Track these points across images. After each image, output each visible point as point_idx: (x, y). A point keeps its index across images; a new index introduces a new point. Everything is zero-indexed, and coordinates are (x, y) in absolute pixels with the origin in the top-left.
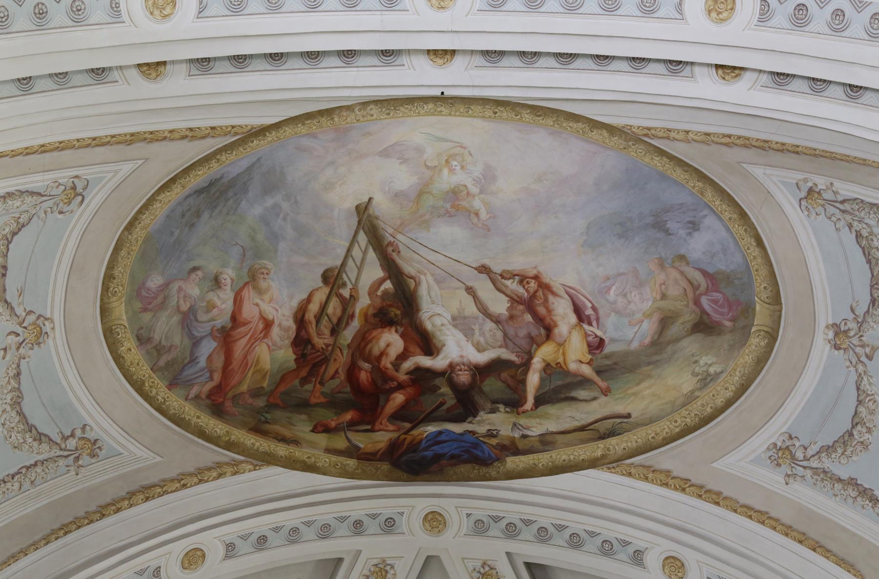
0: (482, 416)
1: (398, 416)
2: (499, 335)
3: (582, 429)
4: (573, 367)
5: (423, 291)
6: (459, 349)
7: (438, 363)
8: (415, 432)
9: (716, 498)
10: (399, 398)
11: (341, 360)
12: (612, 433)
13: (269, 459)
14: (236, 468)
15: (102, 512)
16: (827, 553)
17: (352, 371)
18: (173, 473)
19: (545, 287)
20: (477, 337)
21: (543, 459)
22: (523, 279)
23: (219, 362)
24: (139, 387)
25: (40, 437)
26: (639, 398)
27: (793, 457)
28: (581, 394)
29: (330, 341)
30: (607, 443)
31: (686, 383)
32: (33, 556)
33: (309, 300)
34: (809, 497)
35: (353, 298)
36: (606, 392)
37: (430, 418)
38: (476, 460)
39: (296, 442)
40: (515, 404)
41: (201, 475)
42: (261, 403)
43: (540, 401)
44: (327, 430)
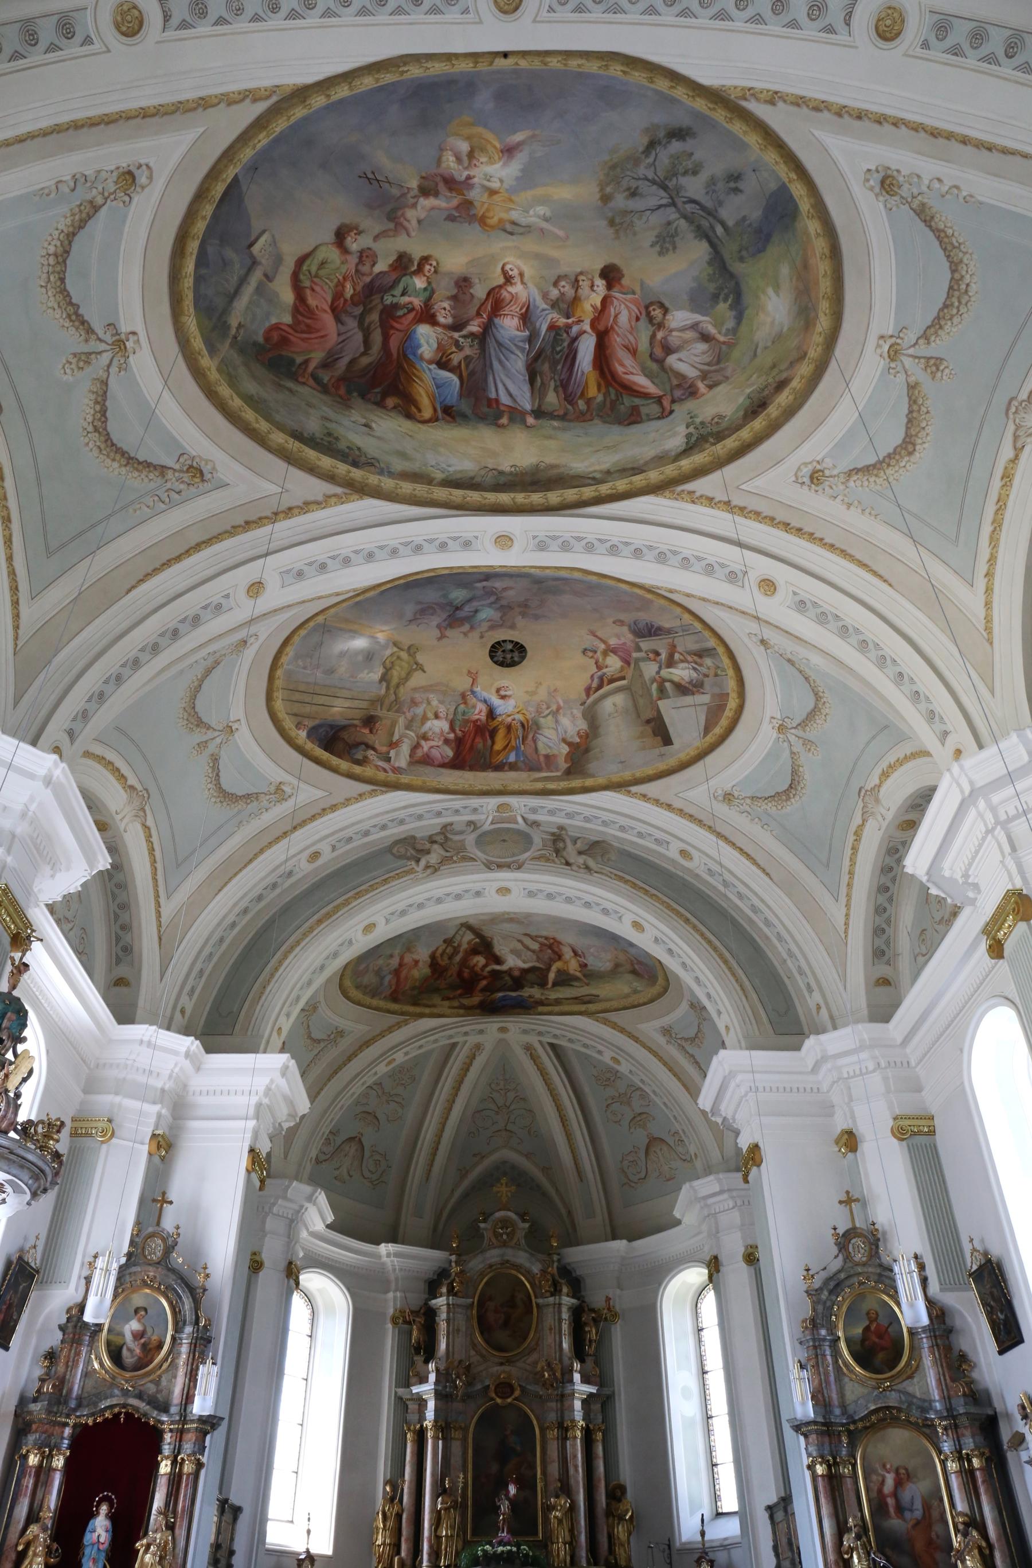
0: (526, 989)
1: (484, 990)
2: (535, 957)
3: (576, 998)
4: (572, 972)
5: (495, 942)
6: (512, 962)
7: (504, 967)
8: (493, 996)
9: (636, 1040)
10: (484, 983)
11: (454, 970)
12: (589, 1002)
13: (422, 1016)
14: (406, 1023)
15: (349, 1059)
16: (679, 1079)
17: (460, 974)
18: (378, 1032)
19: (559, 943)
20: (523, 957)
21: (557, 1009)
22: (546, 938)
23: (394, 982)
24: (359, 1003)
25: (319, 1041)
27: (671, 1035)
28: (575, 984)
29: (447, 962)
30: (585, 1005)
31: (626, 990)
32: (325, 1089)
33: (437, 949)
34: (673, 1051)
35: (459, 946)
36: (587, 985)
37: (499, 990)
38: (523, 1007)
39: (434, 1006)
40: (543, 984)
41: (390, 1030)
42: (415, 992)
43: (554, 985)
44: (448, 999)
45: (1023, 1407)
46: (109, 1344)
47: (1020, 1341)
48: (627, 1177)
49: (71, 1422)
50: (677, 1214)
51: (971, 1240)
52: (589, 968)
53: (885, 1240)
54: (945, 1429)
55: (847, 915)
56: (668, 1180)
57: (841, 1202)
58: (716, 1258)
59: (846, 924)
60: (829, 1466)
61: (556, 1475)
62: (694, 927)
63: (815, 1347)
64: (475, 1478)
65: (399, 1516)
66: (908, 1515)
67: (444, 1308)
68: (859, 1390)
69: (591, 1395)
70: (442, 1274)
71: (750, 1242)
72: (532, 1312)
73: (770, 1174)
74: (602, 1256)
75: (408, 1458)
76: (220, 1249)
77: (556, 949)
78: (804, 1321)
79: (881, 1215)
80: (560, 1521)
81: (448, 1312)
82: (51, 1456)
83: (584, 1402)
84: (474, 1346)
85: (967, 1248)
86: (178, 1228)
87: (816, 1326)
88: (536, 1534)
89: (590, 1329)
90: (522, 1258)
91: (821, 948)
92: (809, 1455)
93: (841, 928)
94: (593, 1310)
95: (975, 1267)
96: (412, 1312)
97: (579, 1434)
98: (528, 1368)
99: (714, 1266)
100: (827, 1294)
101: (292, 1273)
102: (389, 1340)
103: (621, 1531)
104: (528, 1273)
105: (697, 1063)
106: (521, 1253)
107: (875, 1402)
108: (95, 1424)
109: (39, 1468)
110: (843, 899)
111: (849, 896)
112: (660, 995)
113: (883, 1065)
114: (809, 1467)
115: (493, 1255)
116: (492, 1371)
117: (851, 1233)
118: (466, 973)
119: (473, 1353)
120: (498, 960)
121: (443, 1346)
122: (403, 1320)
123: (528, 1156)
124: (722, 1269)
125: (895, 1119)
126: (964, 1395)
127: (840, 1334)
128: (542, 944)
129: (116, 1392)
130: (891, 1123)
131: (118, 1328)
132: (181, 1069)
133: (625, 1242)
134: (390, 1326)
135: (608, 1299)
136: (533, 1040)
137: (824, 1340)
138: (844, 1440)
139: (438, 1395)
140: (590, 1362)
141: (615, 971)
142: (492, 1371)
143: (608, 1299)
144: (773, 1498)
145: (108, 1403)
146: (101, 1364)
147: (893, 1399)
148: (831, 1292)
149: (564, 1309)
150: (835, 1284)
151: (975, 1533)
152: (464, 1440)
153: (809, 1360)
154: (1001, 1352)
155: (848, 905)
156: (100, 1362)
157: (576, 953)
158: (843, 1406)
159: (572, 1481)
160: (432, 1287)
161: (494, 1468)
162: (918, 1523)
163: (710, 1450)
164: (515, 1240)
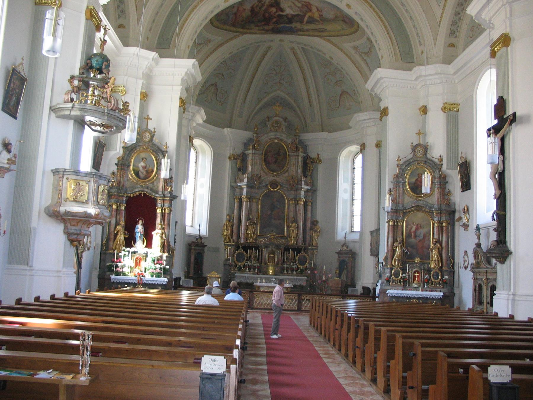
0: (294, 24)
1: (274, 23)
3: (316, 29)
6: (288, 11)
7: (285, 14)
9: (342, 50)
10: (275, 20)
13: (246, 33)
14: (238, 36)
17: (264, 15)
19: (311, 5)
21: (307, 33)
22: (305, 2)
24: (218, 27)
26: (330, 27)
30: (320, 33)
31: (339, 28)
34: (357, 57)
35: (265, 3)
36: (322, 24)
37: (282, 23)
38: (292, 31)
39: (251, 29)
40: (301, 22)
41: (231, 39)
43: (307, 22)
44: (258, 26)
45: (464, 209)
46: (134, 170)
47: (470, 189)
48: (331, 106)
49: (125, 196)
50: (350, 124)
51: (462, 153)
52: (323, 16)
53: (430, 149)
54: (437, 214)
55: (442, 14)
56: (348, 109)
57: (416, 134)
58: (364, 144)
59: (441, 18)
60: (394, 222)
61: (292, 216)
62: (374, 10)
63: (397, 184)
64: (261, 216)
65: (232, 226)
66: (417, 238)
67: (251, 155)
68: (409, 200)
69: (308, 190)
70: (250, 140)
71: (379, 139)
72: (286, 158)
73: (391, 119)
74: (317, 141)
75: (236, 207)
76: (170, 137)
77: (309, 7)
78: (394, 175)
79: (430, 140)
80: (293, 231)
81: (252, 156)
82: (120, 206)
83: (305, 192)
84: (262, 169)
85: (460, 156)
86: (155, 129)
87: (398, 179)
88: (284, 234)
89: (309, 165)
90: (283, 136)
91: (429, 27)
92: (388, 218)
93: (438, 19)
94: (311, 158)
95: (461, 163)
96: (238, 155)
97: (302, 203)
98: (284, 178)
99: (363, 148)
100: (404, 166)
101: (191, 140)
102: (228, 165)
103: (315, 235)
104: (285, 143)
105: (367, 63)
106: (283, 135)
107: (414, 204)
108: (134, 197)
109: (117, 210)
110: (442, 6)
111: (445, 5)
112: (354, 32)
113: (444, 81)
114: (387, 222)
115: (272, 135)
116: (269, 178)
117: (419, 145)
118: (267, 15)
119: (262, 172)
120: (282, 10)
121: (250, 169)
122: (234, 158)
123: (288, 94)
124: (366, 148)
125: (444, 104)
126: (446, 204)
127: (407, 180)
128: (303, 5)
129: (139, 186)
130: (442, 105)
131: (136, 164)
132: (151, 65)
133: (327, 133)
134: (228, 161)
135: (318, 155)
136: (296, 46)
137: (401, 182)
138: (401, 215)
139: (248, 186)
140: (309, 178)
141: (335, 19)
142: (269, 178)
143: (318, 155)
144: (373, 229)
145: (137, 190)
146: (132, 177)
147: (421, 203)
148: (406, 166)
149: (300, 158)
150: (408, 163)
151: (438, 245)
152: (258, 203)
153: (394, 188)
154: (462, 192)
155: (443, 9)
156: (131, 175)
157: (318, 10)
158: (403, 204)
159: (299, 219)
160: (245, 146)
161: (269, 212)
162: (420, 241)
163: (352, 211)
164: (281, 129)
